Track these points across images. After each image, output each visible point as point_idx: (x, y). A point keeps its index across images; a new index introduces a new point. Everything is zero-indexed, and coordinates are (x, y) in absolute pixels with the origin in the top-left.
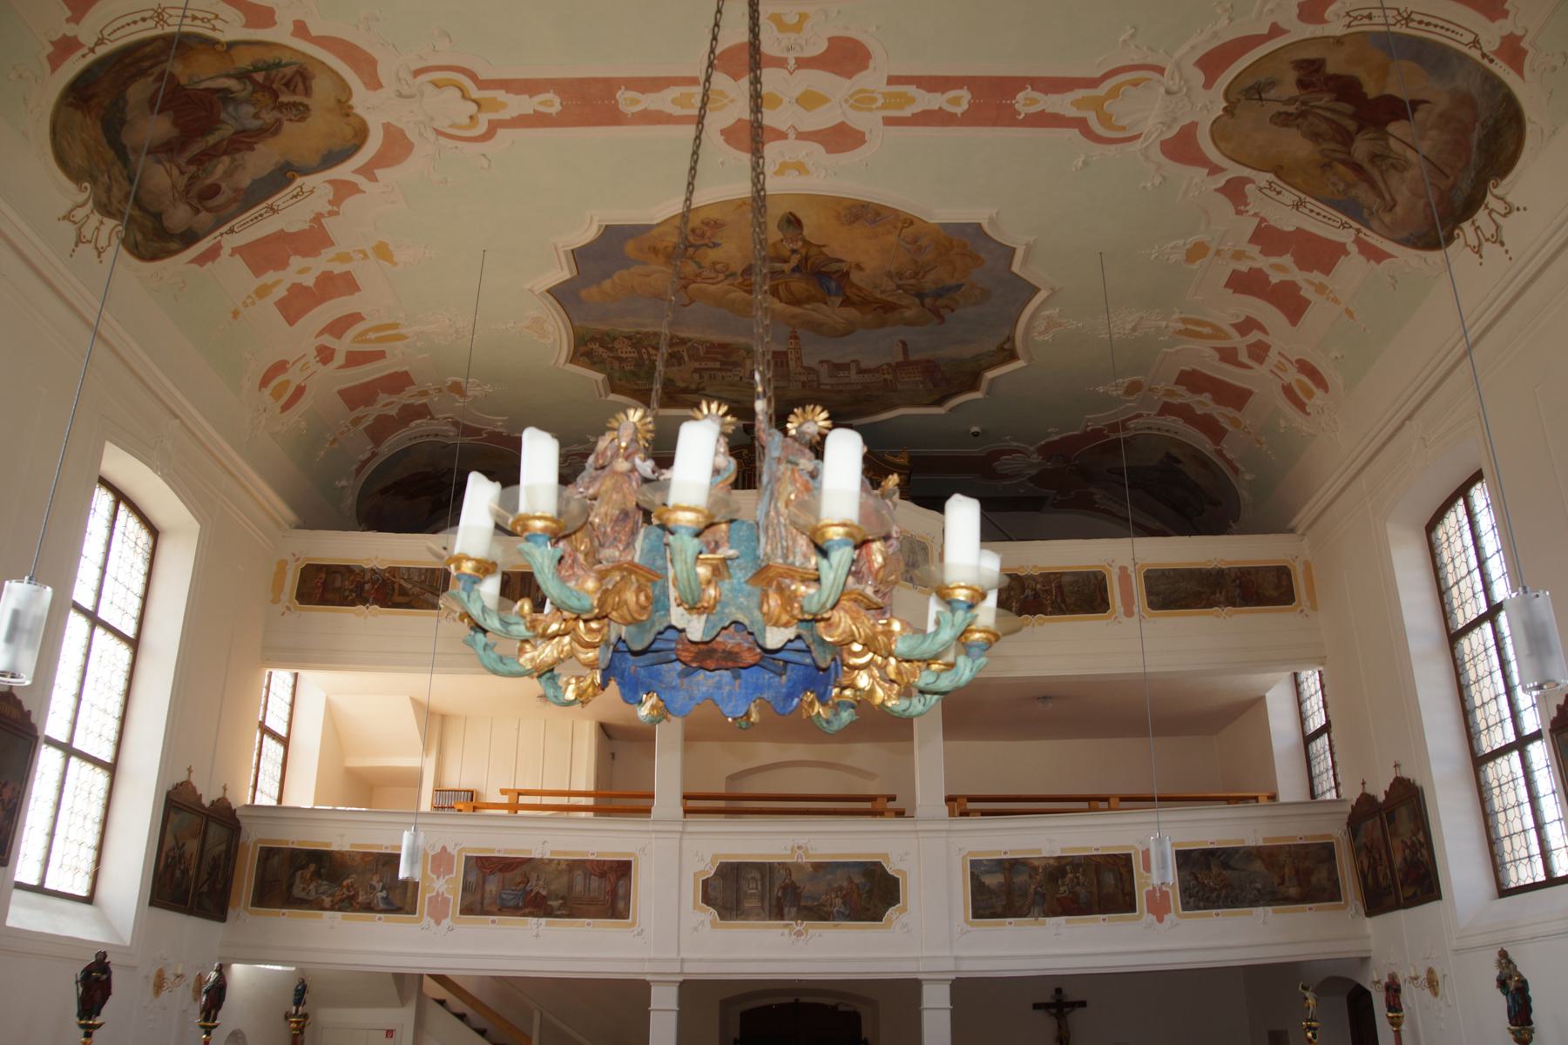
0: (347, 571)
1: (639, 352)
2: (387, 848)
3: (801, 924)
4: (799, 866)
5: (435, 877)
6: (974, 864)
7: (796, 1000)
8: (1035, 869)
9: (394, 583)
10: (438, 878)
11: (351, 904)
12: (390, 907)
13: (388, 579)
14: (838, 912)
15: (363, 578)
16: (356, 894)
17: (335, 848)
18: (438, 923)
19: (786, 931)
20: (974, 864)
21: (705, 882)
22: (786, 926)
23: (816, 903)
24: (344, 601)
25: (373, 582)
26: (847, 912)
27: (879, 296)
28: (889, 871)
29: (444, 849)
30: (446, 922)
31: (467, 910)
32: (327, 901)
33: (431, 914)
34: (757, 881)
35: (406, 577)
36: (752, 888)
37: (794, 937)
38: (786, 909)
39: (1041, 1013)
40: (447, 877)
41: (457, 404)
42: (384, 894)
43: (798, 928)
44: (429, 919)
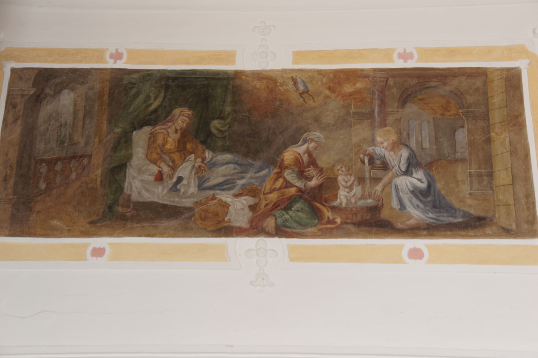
2: (405, 56)
11: (316, 214)
12: (446, 219)
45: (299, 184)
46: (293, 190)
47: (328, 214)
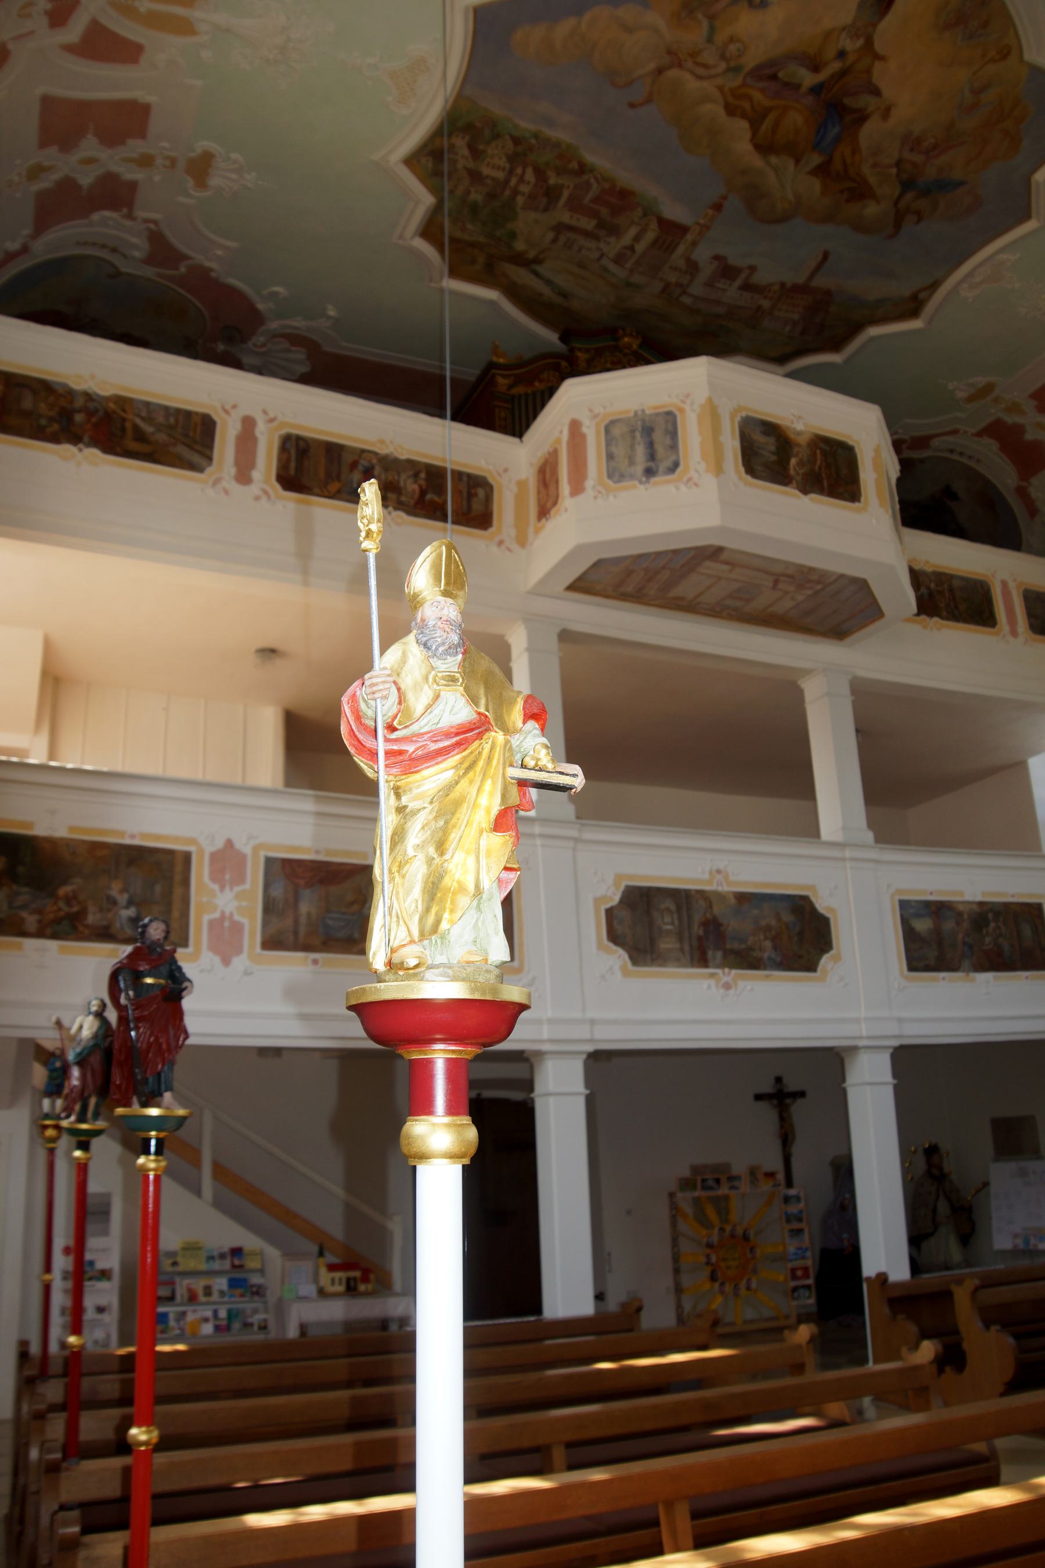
0: (43, 388)
1: (511, 172)
2: (133, 836)
3: (729, 974)
4: (720, 896)
5: (216, 887)
6: (904, 904)
7: (479, 1095)
8: (960, 914)
9: (124, 420)
10: (222, 889)
11: (75, 928)
13: (114, 412)
14: (769, 958)
15: (72, 402)
16: (82, 913)
17: (41, 829)
18: (226, 962)
19: (712, 982)
20: (904, 904)
21: (609, 912)
22: (712, 975)
23: (743, 946)
24: (39, 434)
25: (90, 414)
26: (779, 959)
27: (866, 170)
29: (229, 843)
30: (240, 962)
31: (272, 943)
32: (31, 921)
33: (214, 948)
35: (144, 414)
36: (667, 923)
37: (722, 991)
38: (710, 953)
39: (763, 1105)
40: (237, 889)
41: (182, 199)
42: (131, 912)
43: (726, 979)
44: (210, 955)
45: (66, 909)
46: (62, 914)
47: (81, 928)
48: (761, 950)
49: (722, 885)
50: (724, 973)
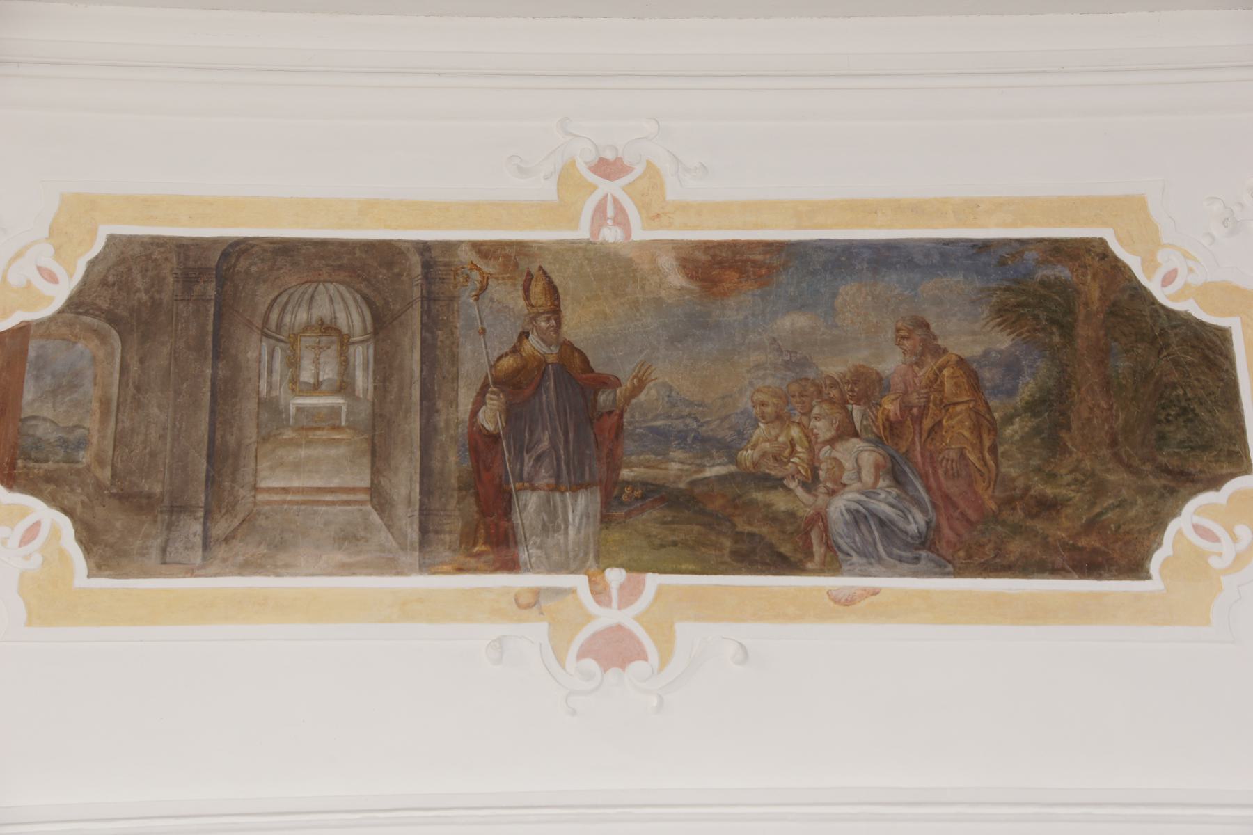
3: (629, 594)
14: (858, 518)
22: (532, 602)
26: (916, 523)
28: (1162, 295)
34: (345, 342)
38: (529, 506)
43: (606, 617)
48: (811, 483)
49: (621, 219)
50: (599, 592)
